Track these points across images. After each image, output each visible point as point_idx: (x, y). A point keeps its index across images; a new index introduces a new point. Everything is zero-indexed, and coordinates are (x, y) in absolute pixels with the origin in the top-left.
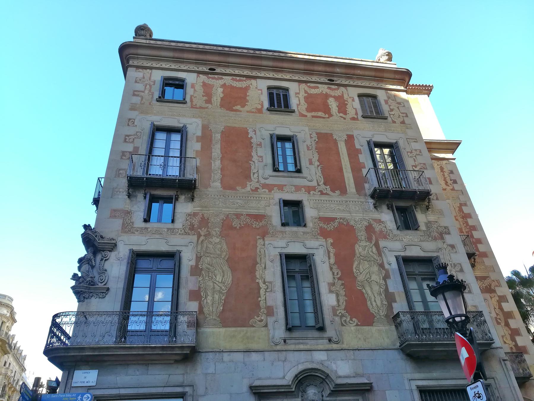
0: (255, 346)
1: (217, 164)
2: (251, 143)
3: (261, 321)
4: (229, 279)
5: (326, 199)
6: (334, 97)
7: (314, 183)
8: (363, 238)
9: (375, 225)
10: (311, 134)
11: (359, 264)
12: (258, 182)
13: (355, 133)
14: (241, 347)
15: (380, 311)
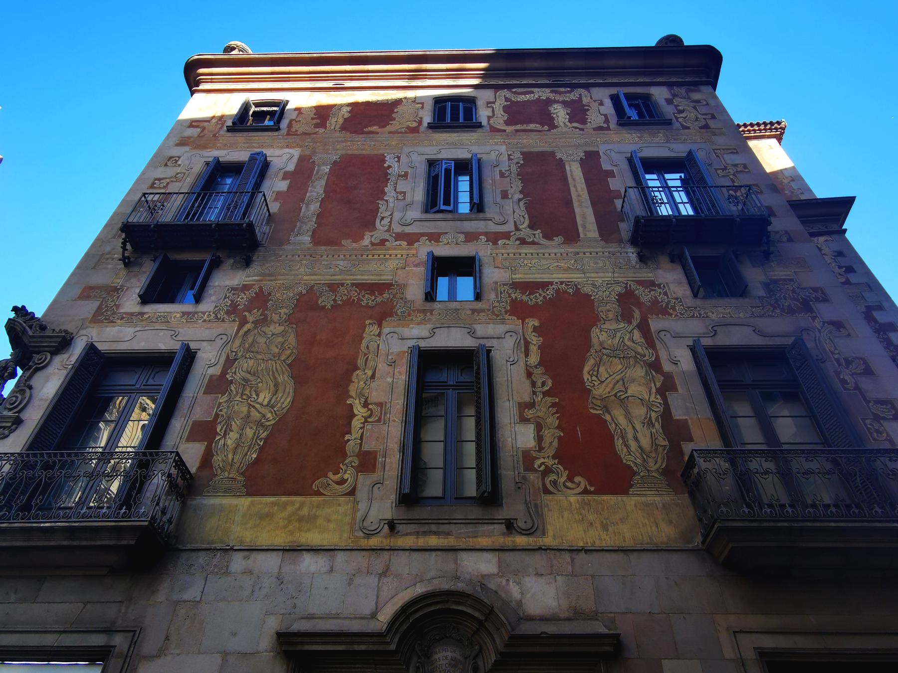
0: (314, 538)
2: (387, 174)
3: (342, 482)
5: (531, 251)
6: (565, 104)
7: (509, 227)
8: (611, 315)
9: (640, 291)
10: (509, 156)
11: (598, 365)
12: (388, 231)
13: (602, 149)
14: (281, 539)
15: (650, 460)
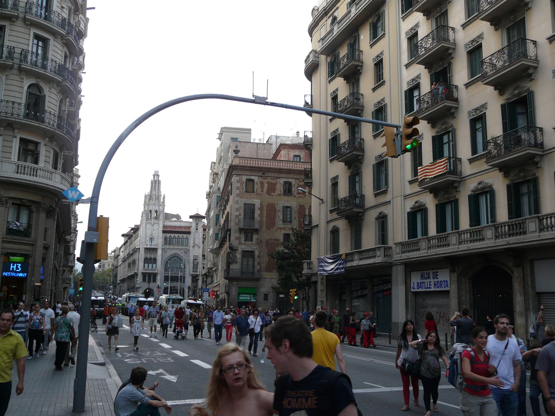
1: (265, 220)
4: (267, 259)
